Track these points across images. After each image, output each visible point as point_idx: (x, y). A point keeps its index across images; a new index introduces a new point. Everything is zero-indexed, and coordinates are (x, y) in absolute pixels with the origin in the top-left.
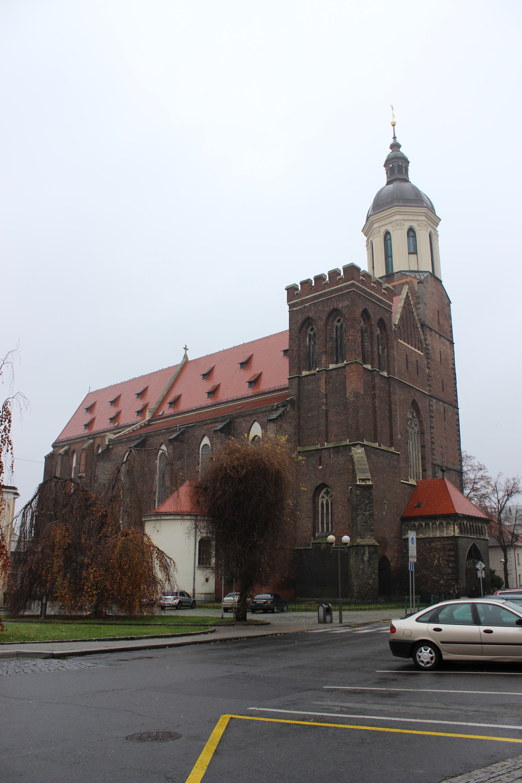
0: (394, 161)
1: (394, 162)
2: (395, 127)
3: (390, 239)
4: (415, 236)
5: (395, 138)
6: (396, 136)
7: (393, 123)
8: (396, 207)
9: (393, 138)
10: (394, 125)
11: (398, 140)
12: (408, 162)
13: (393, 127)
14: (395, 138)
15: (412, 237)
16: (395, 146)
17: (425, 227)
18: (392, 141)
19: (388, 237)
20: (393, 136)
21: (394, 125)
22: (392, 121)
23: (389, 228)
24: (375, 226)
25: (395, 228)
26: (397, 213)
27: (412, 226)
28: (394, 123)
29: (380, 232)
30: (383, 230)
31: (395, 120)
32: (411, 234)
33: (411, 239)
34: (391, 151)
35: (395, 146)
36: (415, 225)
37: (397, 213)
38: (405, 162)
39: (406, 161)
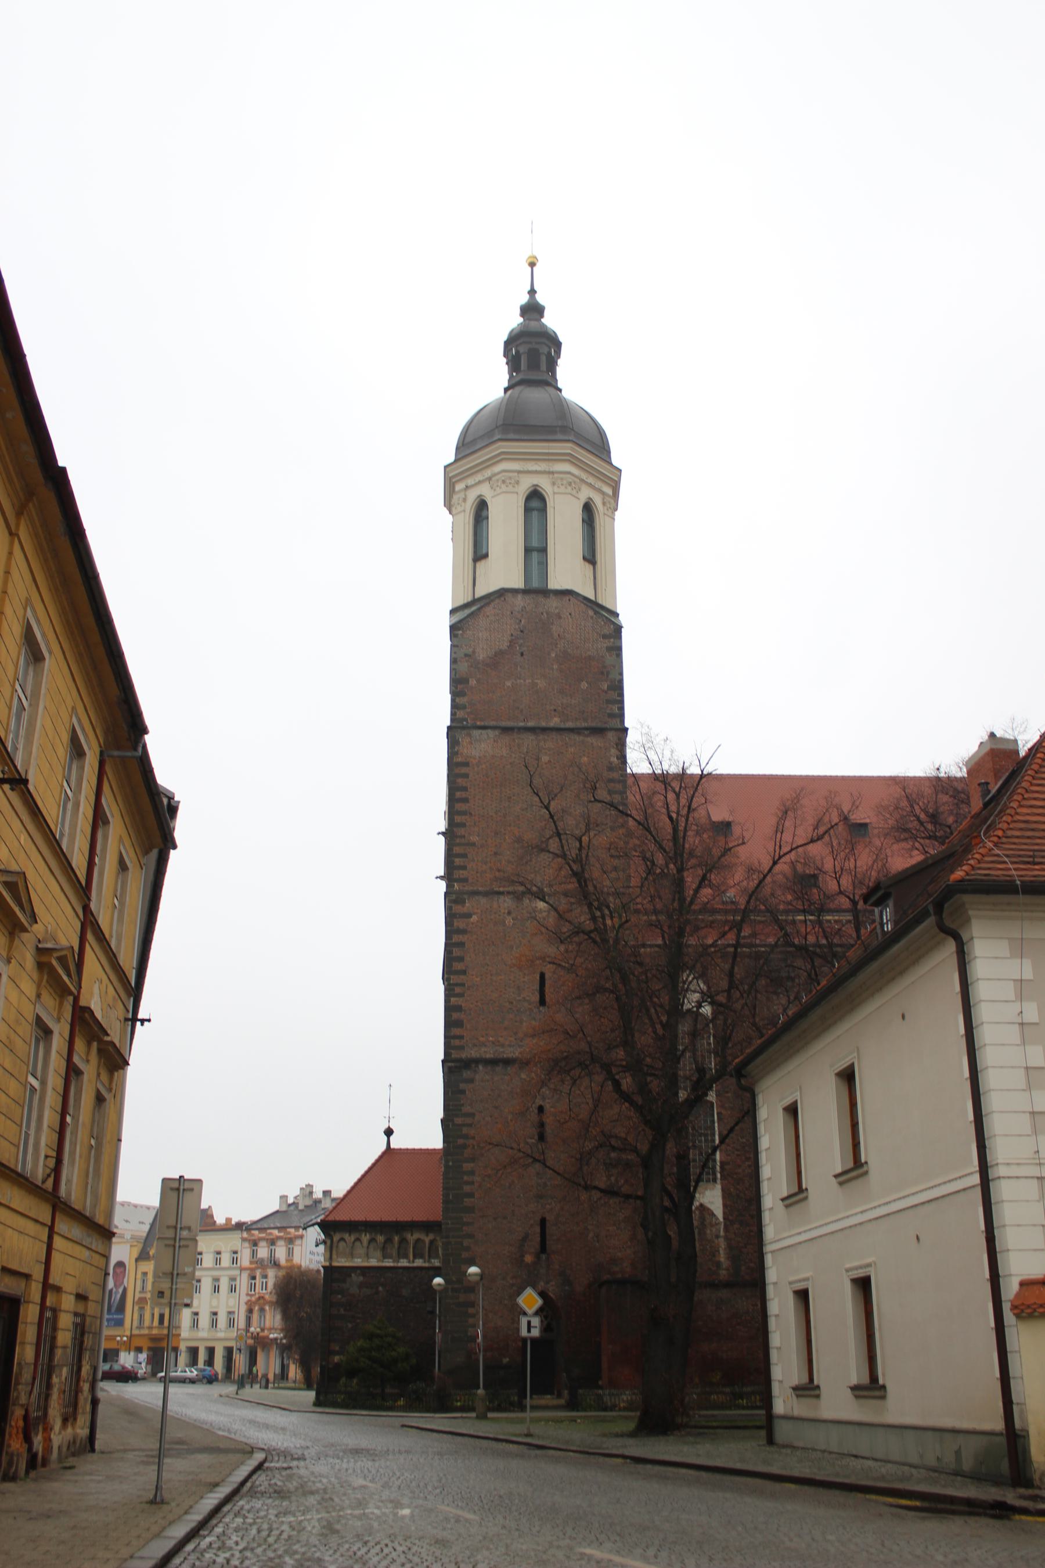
0: (521, 341)
1: (521, 344)
2: (534, 268)
3: (487, 518)
4: (543, 510)
5: (532, 292)
6: (536, 288)
7: (528, 261)
8: (500, 444)
9: (529, 293)
10: (532, 265)
11: (540, 298)
12: (558, 345)
13: (530, 269)
14: (532, 292)
15: (538, 510)
16: (532, 310)
17: (569, 488)
18: (525, 299)
19: (484, 514)
20: (529, 288)
21: (532, 265)
22: (530, 254)
23: (485, 491)
24: (459, 487)
25: (498, 490)
26: (503, 457)
27: (537, 485)
28: (535, 261)
29: (465, 500)
30: (472, 496)
31: (535, 254)
32: (535, 503)
33: (535, 514)
34: (521, 320)
35: (532, 310)
36: (545, 485)
37: (503, 457)
38: (547, 342)
39: (553, 343)
